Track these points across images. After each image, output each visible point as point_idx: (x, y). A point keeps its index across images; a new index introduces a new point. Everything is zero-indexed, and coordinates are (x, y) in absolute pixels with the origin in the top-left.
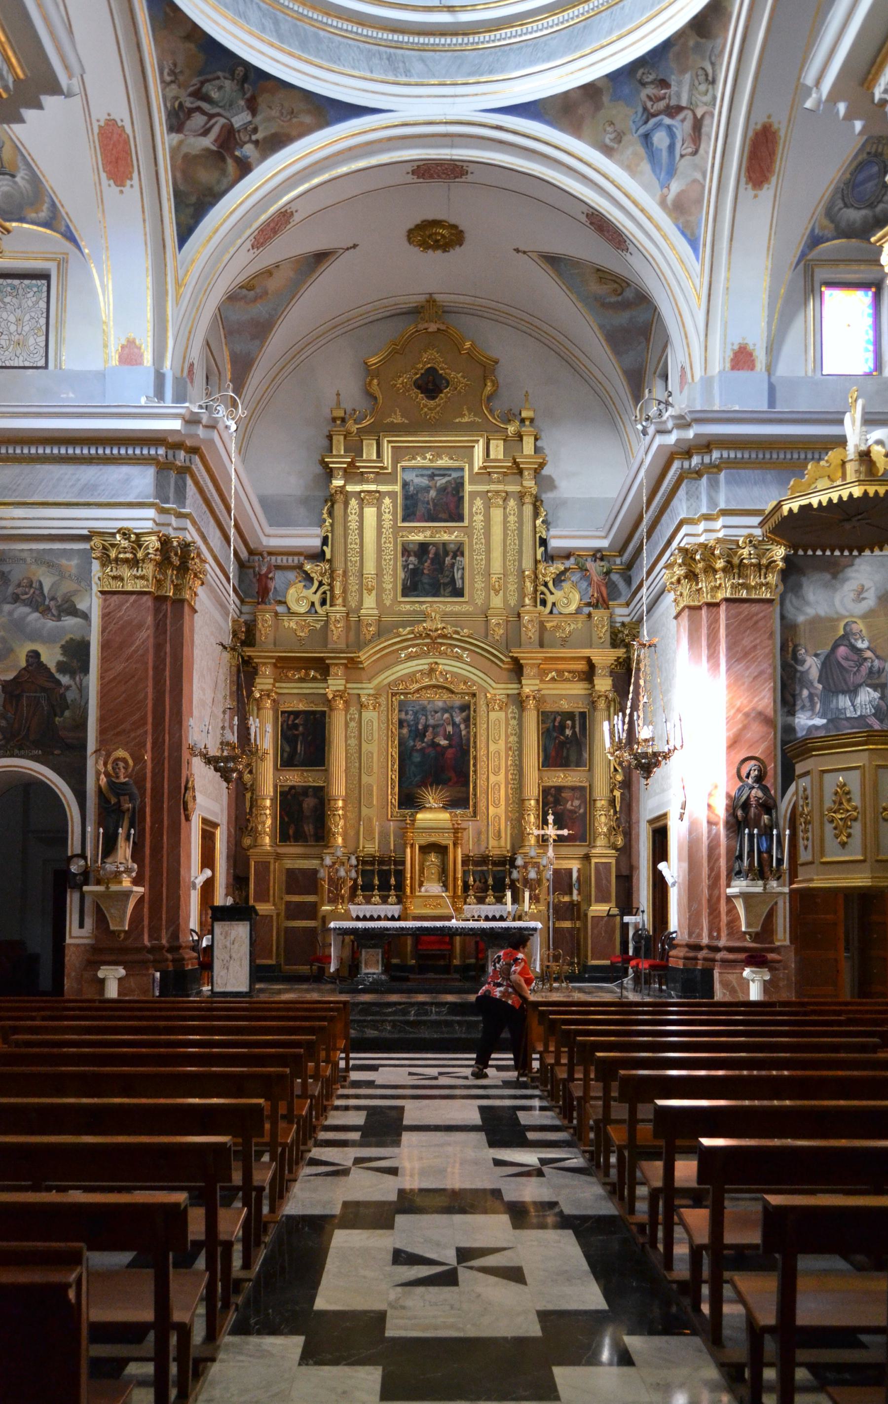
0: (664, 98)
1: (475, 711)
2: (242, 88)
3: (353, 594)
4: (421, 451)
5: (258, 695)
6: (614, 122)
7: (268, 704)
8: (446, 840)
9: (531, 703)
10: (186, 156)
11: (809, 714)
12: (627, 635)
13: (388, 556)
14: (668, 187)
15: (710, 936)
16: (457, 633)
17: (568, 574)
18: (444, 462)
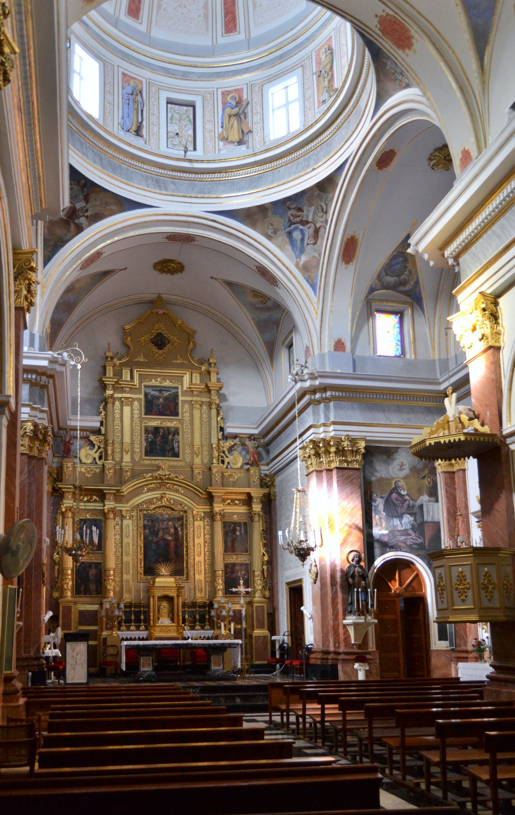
0: (300, 216)
1: (186, 521)
2: (83, 189)
3: (117, 454)
4: (155, 377)
5: (64, 510)
6: (273, 224)
7: (70, 515)
8: (173, 593)
9: (218, 517)
11: (379, 528)
12: (269, 481)
13: (137, 433)
14: (300, 258)
15: (335, 646)
16: (177, 477)
17: (236, 447)
18: (167, 383)
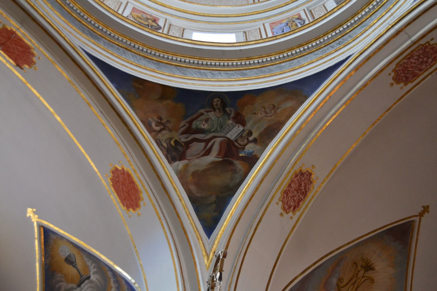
2: (225, 112)
10: (195, 174)
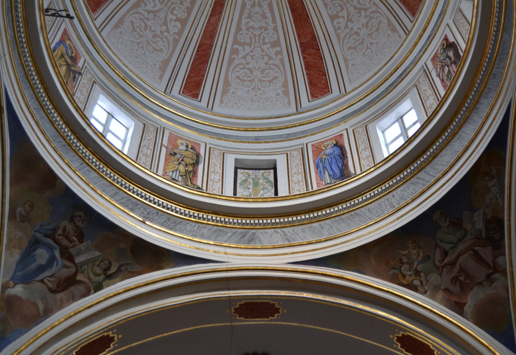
0: (71, 242)
14: (15, 284)
